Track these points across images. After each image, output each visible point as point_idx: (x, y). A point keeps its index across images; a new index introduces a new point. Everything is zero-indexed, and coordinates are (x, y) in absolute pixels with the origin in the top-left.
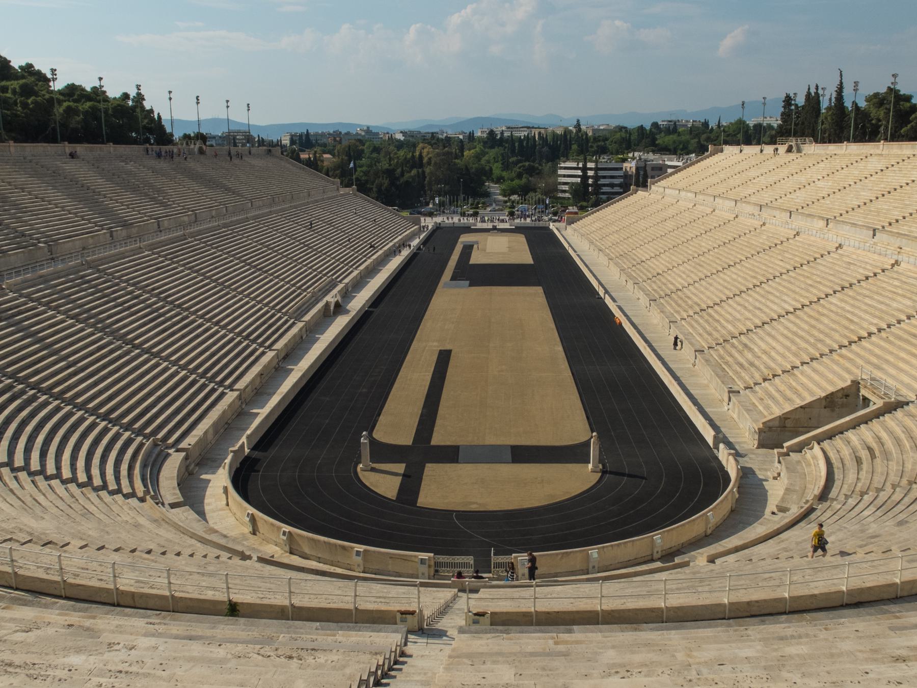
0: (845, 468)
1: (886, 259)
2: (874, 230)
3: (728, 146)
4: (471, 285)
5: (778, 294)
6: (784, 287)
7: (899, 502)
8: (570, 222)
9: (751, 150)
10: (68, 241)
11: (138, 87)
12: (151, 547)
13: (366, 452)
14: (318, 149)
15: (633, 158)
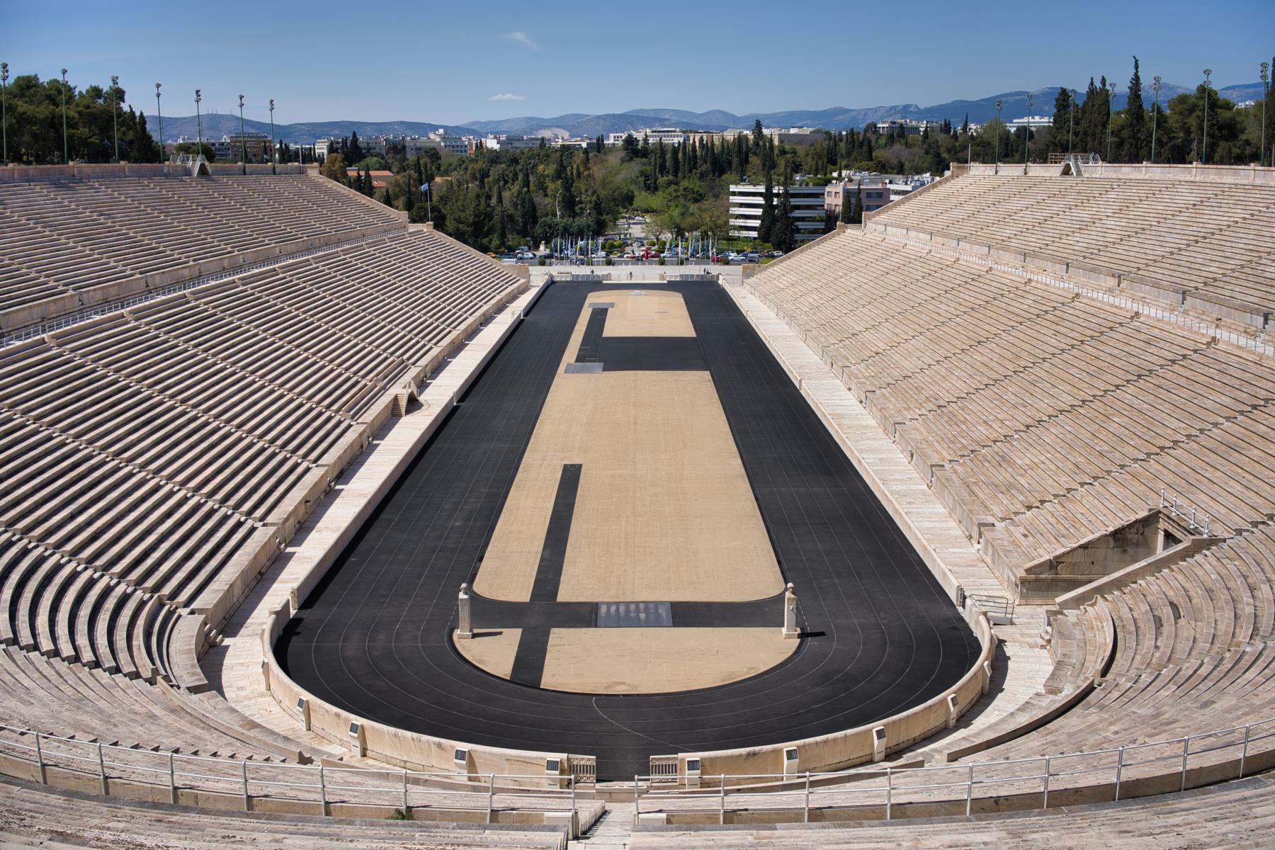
0: (1140, 633)
3: (977, 164)
4: (605, 369)
8: (747, 274)
9: (1010, 171)
10: (24, 309)
11: (115, 80)
12: (178, 746)
13: (464, 614)
14: (372, 160)
15: (840, 178)
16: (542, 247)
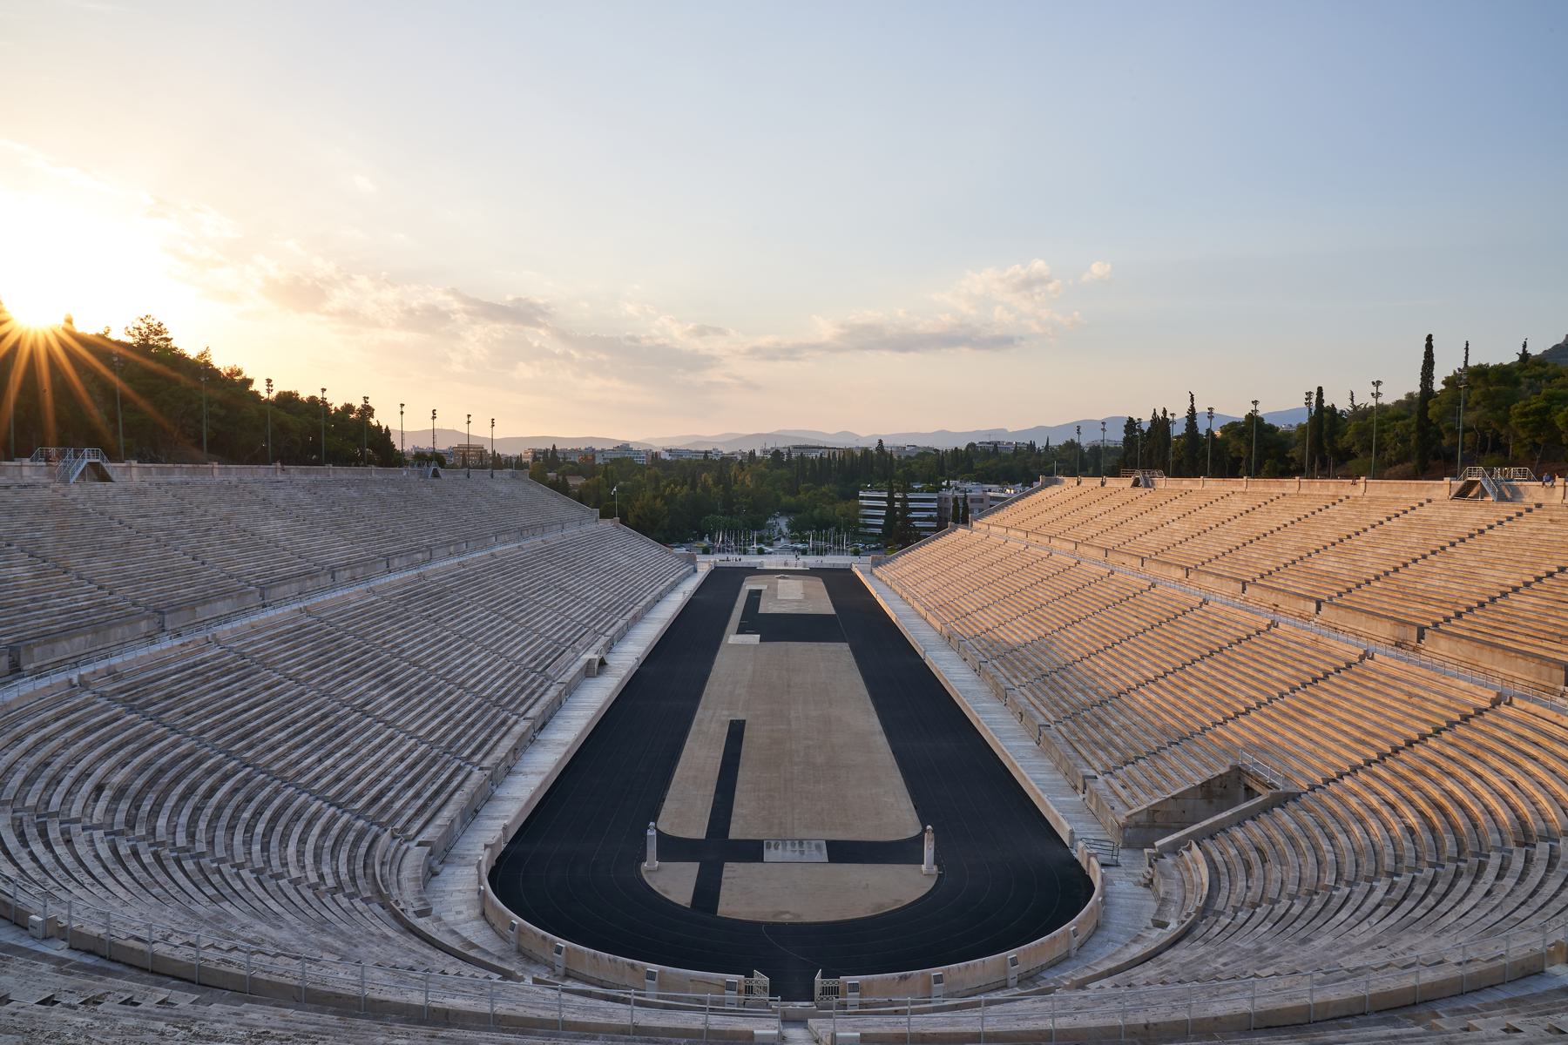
1: (1260, 619)
2: (1244, 583)
5: (1134, 657)
6: (1141, 649)
7: (1299, 917)
16: (707, 539)
